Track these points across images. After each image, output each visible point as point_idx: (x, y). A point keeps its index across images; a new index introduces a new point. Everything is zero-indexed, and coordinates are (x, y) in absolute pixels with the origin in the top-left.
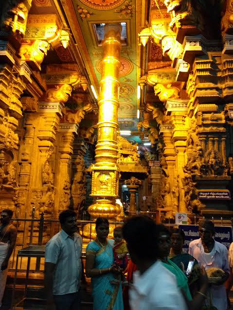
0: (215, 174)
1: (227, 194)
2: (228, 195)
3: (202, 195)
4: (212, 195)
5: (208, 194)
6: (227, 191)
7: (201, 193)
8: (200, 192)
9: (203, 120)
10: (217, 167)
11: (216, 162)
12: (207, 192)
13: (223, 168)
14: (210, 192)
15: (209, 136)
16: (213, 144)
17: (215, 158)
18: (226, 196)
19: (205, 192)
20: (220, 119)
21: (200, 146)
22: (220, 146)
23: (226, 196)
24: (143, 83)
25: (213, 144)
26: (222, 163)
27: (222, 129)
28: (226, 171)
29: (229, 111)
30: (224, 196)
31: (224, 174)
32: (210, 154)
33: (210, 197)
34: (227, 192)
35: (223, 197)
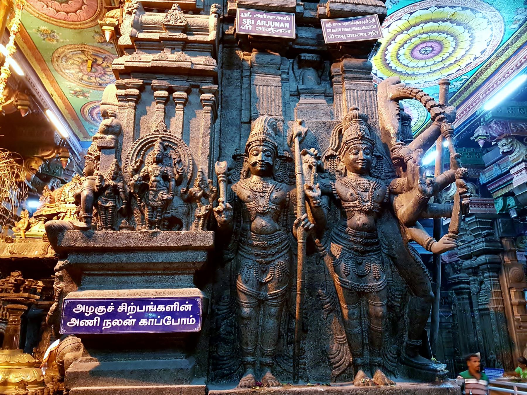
0: (152, 225)
1: (188, 307)
2: (193, 313)
3: (81, 316)
4: (124, 316)
5: (111, 308)
6: (196, 292)
7: (80, 308)
8: (74, 303)
9: (139, 26)
10: (164, 195)
11: (165, 177)
12: (106, 303)
13: (191, 200)
14: (117, 303)
15: (155, 83)
16: (168, 116)
17: (158, 161)
18: (185, 314)
19: (97, 303)
20: (205, 30)
21: (115, 116)
22: (193, 122)
23: (185, 314)
24: (109, 25)
25: (168, 116)
26: (190, 183)
27: (202, 61)
28: (202, 211)
29: (238, 10)
30: (175, 315)
31: (193, 226)
32: (148, 145)
33: (116, 322)
34: (192, 301)
35: (169, 321)
